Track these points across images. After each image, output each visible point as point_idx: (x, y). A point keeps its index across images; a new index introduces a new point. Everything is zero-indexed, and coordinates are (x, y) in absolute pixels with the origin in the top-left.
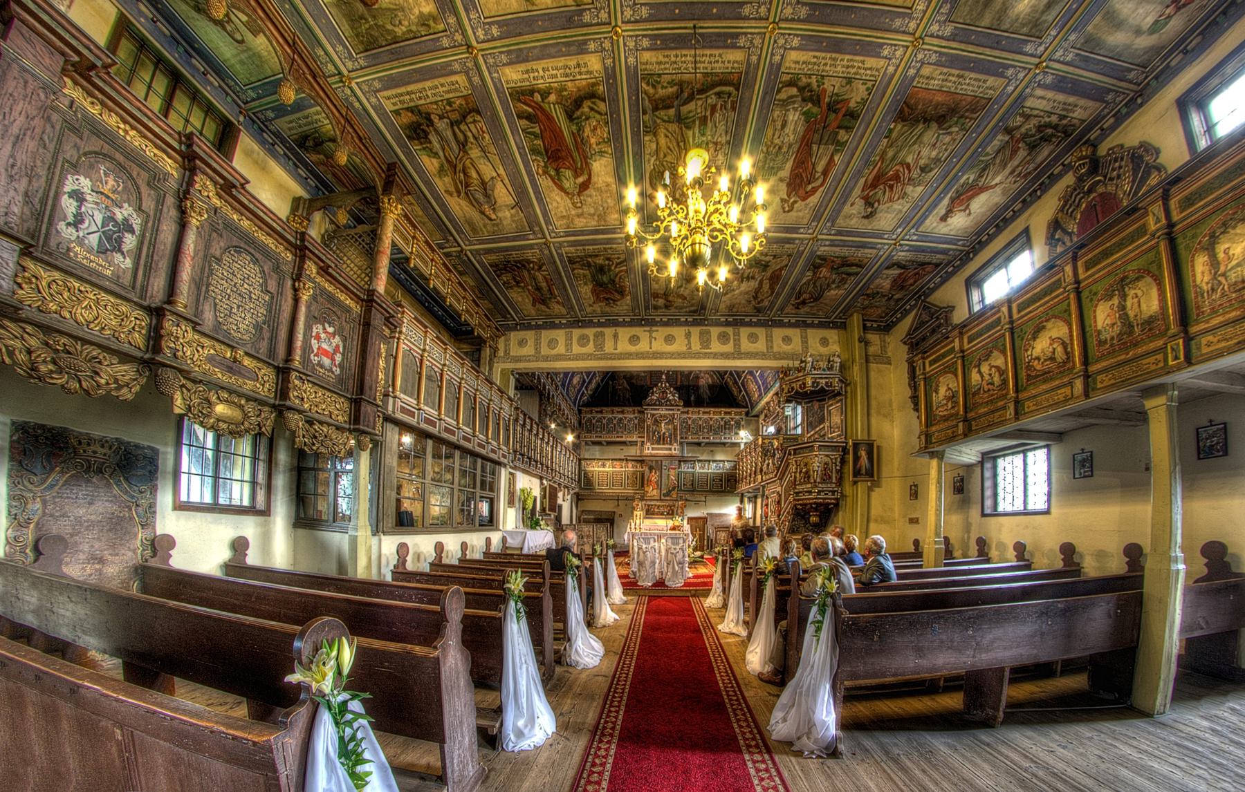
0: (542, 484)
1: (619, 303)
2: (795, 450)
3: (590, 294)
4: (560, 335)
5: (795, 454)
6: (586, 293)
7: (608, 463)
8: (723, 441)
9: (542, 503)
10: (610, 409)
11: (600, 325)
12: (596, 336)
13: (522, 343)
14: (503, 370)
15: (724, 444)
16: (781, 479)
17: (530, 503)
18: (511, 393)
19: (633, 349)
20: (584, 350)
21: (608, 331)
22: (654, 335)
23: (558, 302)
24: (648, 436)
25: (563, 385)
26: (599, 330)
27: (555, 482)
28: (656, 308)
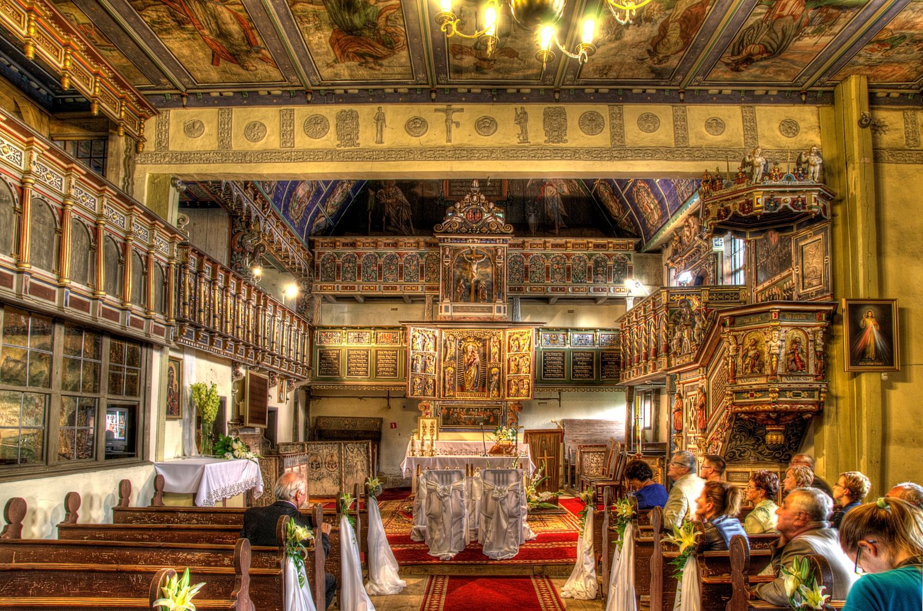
0: (236, 374)
1: (385, 62)
2: (733, 317)
3: (327, 47)
4: (269, 115)
5: (732, 324)
6: (320, 45)
7: (367, 335)
8: (592, 294)
9: (237, 408)
10: (370, 239)
11: (348, 98)
12: (341, 118)
13: (191, 129)
14: (153, 178)
15: (594, 300)
16: (707, 366)
17: (211, 412)
18: (173, 216)
19: (414, 141)
20: (318, 143)
21: (365, 111)
22: (455, 117)
23: (263, 59)
24: (445, 287)
25: (277, 199)
26: (347, 107)
27: (262, 370)
28: (459, 71)
